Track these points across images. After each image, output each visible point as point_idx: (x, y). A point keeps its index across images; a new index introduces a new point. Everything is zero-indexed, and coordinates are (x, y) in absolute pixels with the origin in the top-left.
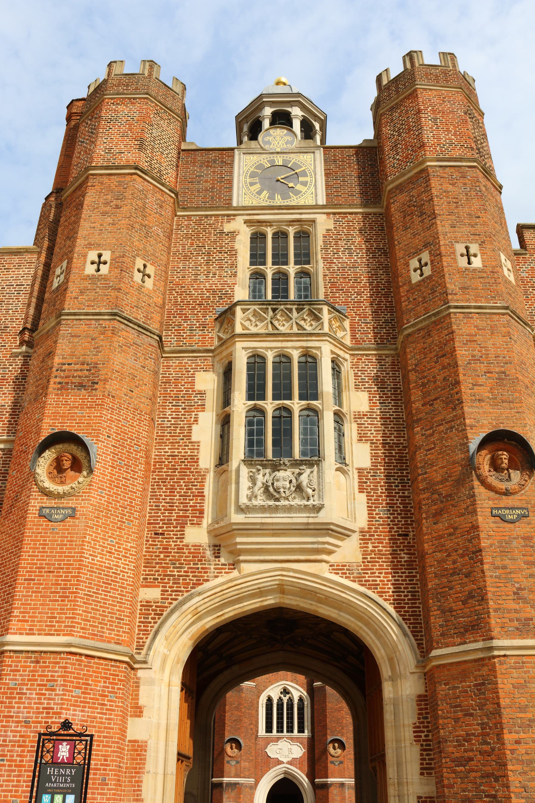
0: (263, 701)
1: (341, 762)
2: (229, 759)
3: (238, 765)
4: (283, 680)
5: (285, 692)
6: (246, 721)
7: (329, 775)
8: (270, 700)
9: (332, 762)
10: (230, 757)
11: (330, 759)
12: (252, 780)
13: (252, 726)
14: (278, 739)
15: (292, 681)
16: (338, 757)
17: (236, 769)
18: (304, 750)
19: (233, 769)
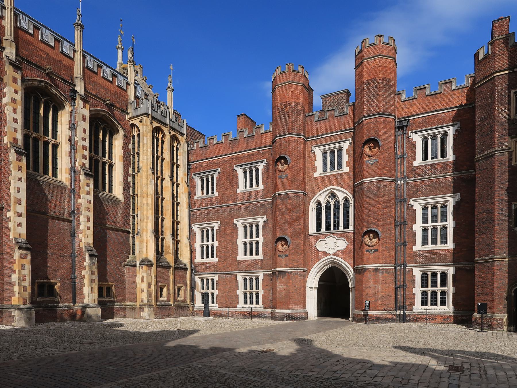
0: (313, 206)
1: (376, 250)
2: (280, 253)
3: (287, 257)
4: (330, 185)
5: (333, 195)
7: (365, 261)
8: (319, 203)
9: (367, 251)
11: (366, 248)
12: (301, 269)
13: (300, 227)
14: (325, 235)
15: (338, 186)
16: (373, 246)
17: (286, 261)
18: (347, 243)
19: (283, 261)
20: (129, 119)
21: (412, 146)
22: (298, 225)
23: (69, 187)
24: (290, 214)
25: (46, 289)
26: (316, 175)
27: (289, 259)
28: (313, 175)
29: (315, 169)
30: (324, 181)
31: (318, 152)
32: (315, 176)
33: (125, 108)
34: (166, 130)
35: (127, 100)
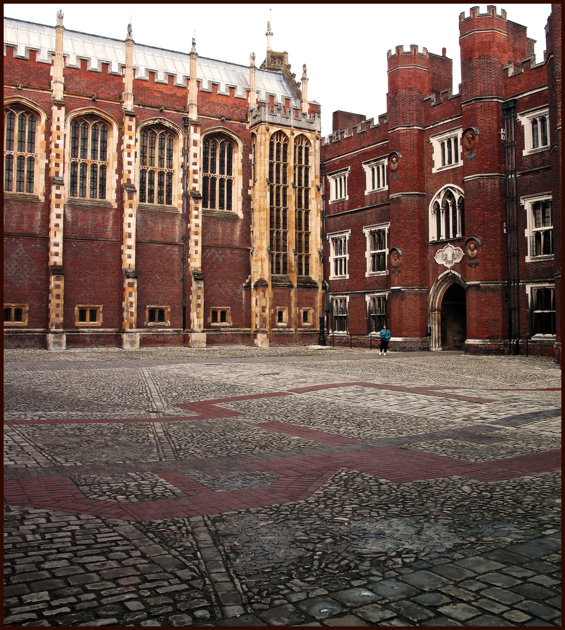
3: (400, 274)
5: (449, 195)
6: (407, 231)
10: (394, 267)
20: (250, 128)
21: (520, 129)
22: (412, 234)
23: (181, 212)
24: (402, 221)
25: (157, 314)
26: (434, 171)
27: (401, 276)
28: (431, 171)
29: (432, 164)
30: (443, 177)
31: (435, 142)
32: (433, 172)
33: (245, 118)
34: (288, 132)
35: (248, 108)
